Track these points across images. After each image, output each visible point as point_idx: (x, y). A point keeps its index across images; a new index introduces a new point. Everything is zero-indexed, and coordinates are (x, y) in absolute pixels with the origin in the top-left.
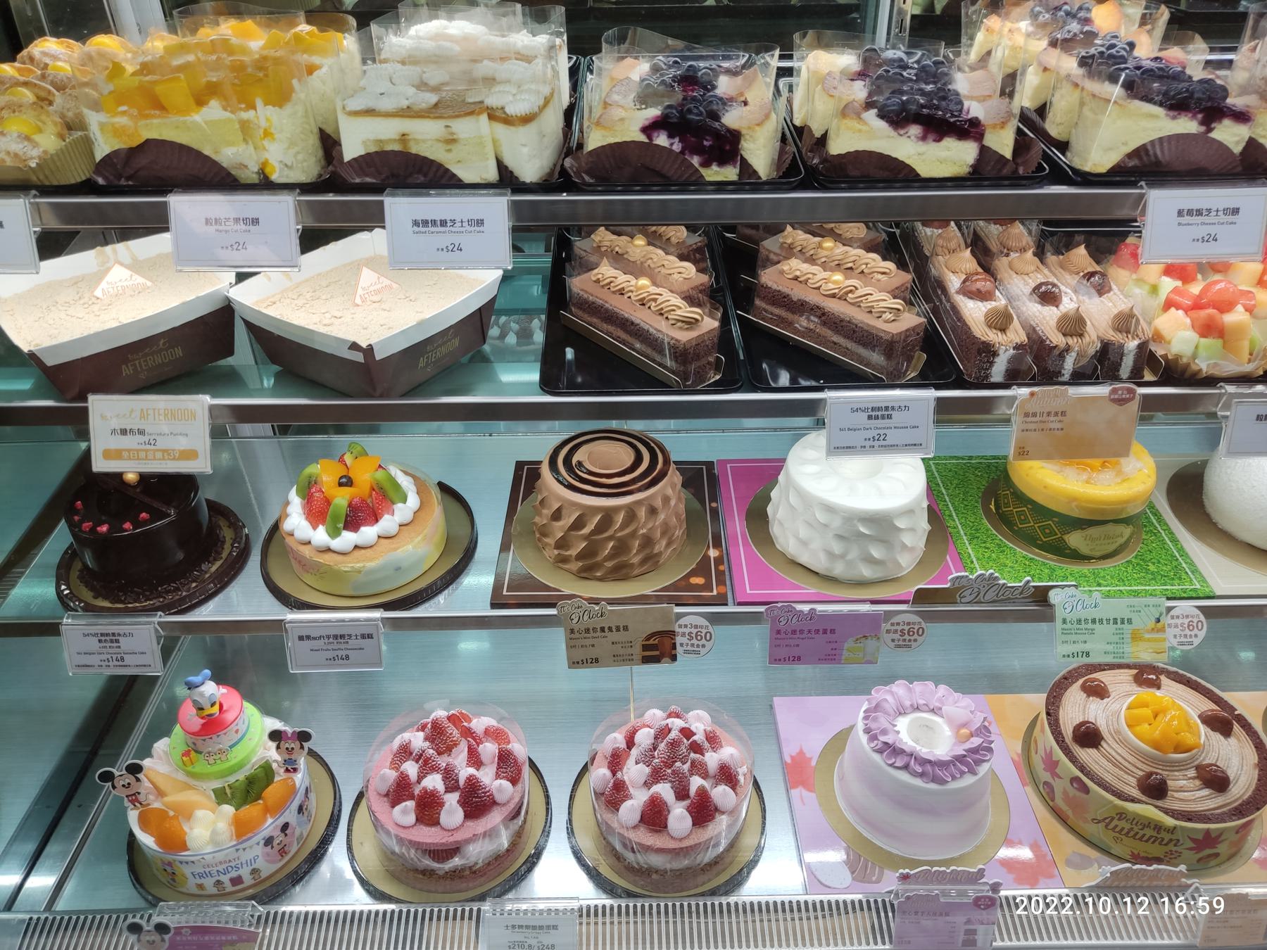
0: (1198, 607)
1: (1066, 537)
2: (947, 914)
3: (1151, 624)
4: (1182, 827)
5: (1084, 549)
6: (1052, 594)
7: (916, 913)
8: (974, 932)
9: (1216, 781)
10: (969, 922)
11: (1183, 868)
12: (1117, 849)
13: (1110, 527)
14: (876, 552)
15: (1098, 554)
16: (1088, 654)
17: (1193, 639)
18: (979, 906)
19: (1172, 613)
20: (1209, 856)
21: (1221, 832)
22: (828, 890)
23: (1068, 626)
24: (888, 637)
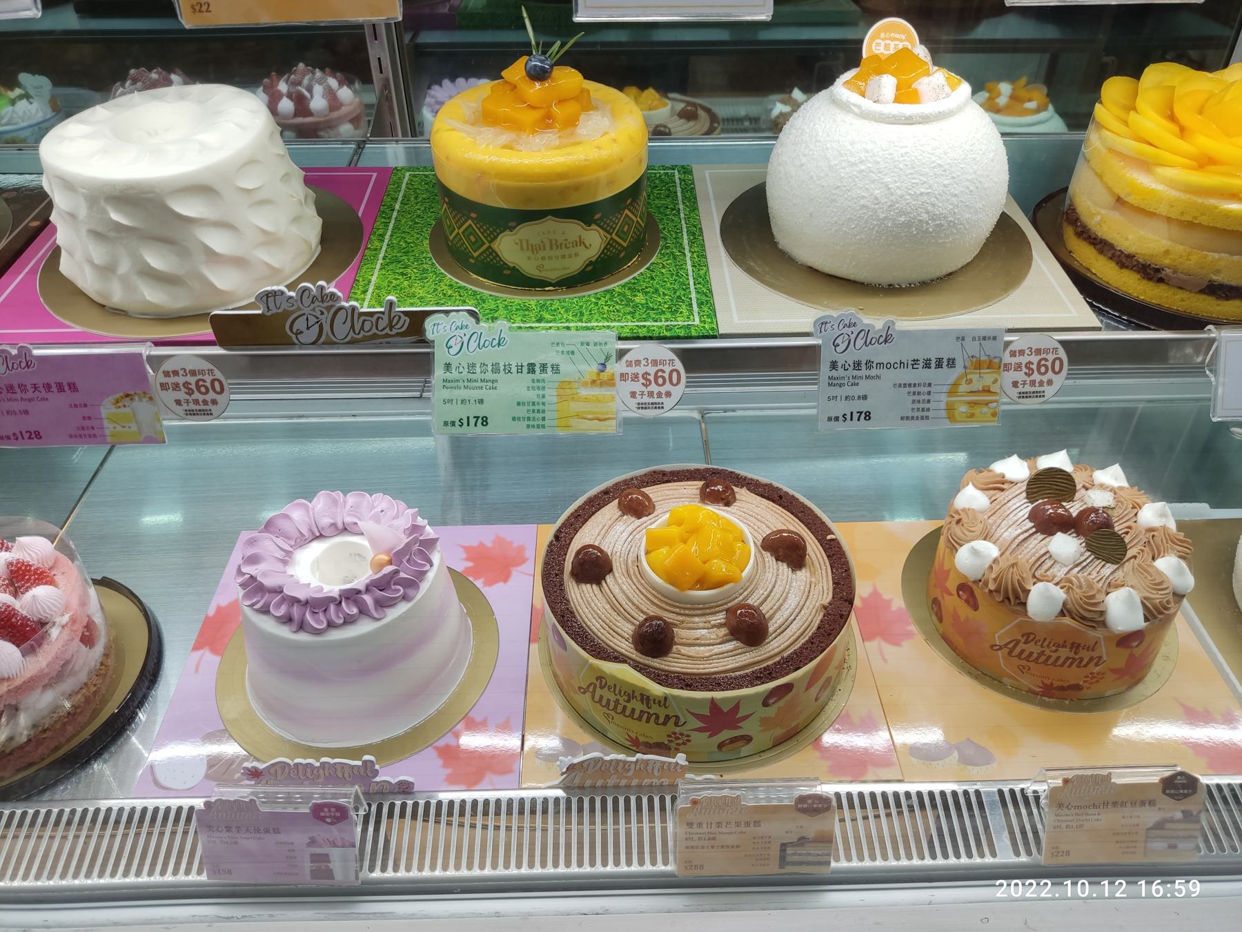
0: (673, 350)
1: (495, 246)
2: (276, 831)
3: (591, 369)
4: (674, 697)
5: (529, 267)
6: (429, 324)
7: (228, 829)
8: (325, 858)
9: (749, 628)
10: (313, 842)
11: (681, 759)
12: (612, 732)
13: (550, 224)
14: (156, 260)
15: (553, 276)
16: (485, 421)
17: (664, 399)
18: (323, 819)
19: (627, 357)
20: (733, 740)
21: (737, 704)
22: (162, 793)
23: (454, 374)
24: (169, 396)
